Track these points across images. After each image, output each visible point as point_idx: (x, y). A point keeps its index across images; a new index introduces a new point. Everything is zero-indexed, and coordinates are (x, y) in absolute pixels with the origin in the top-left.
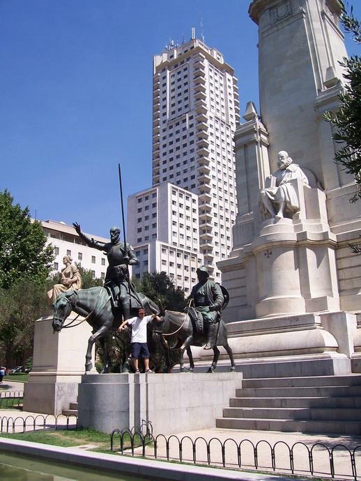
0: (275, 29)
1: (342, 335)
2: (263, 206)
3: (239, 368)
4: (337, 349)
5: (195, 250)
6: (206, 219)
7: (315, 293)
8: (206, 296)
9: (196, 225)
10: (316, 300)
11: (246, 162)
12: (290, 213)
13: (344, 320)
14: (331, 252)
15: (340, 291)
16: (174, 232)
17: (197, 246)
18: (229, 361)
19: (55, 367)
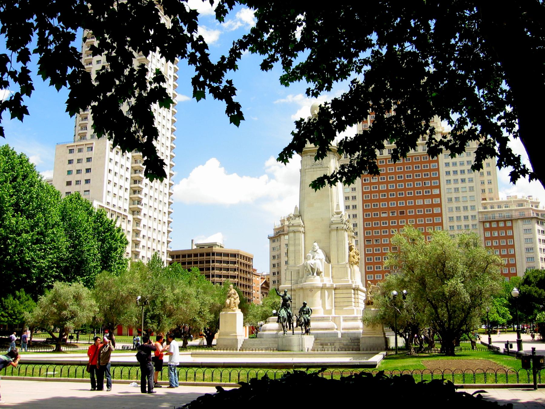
0: (312, 170)
1: (339, 325)
2: (307, 267)
3: (313, 334)
4: (337, 329)
5: (125, 210)
6: (137, 179)
7: (328, 307)
8: (306, 311)
9: (127, 185)
10: (328, 310)
11: (295, 239)
12: (318, 274)
13: (340, 319)
14: (333, 291)
15: (335, 306)
16: (108, 192)
17: (127, 206)
18: (301, 331)
19: (236, 333)
